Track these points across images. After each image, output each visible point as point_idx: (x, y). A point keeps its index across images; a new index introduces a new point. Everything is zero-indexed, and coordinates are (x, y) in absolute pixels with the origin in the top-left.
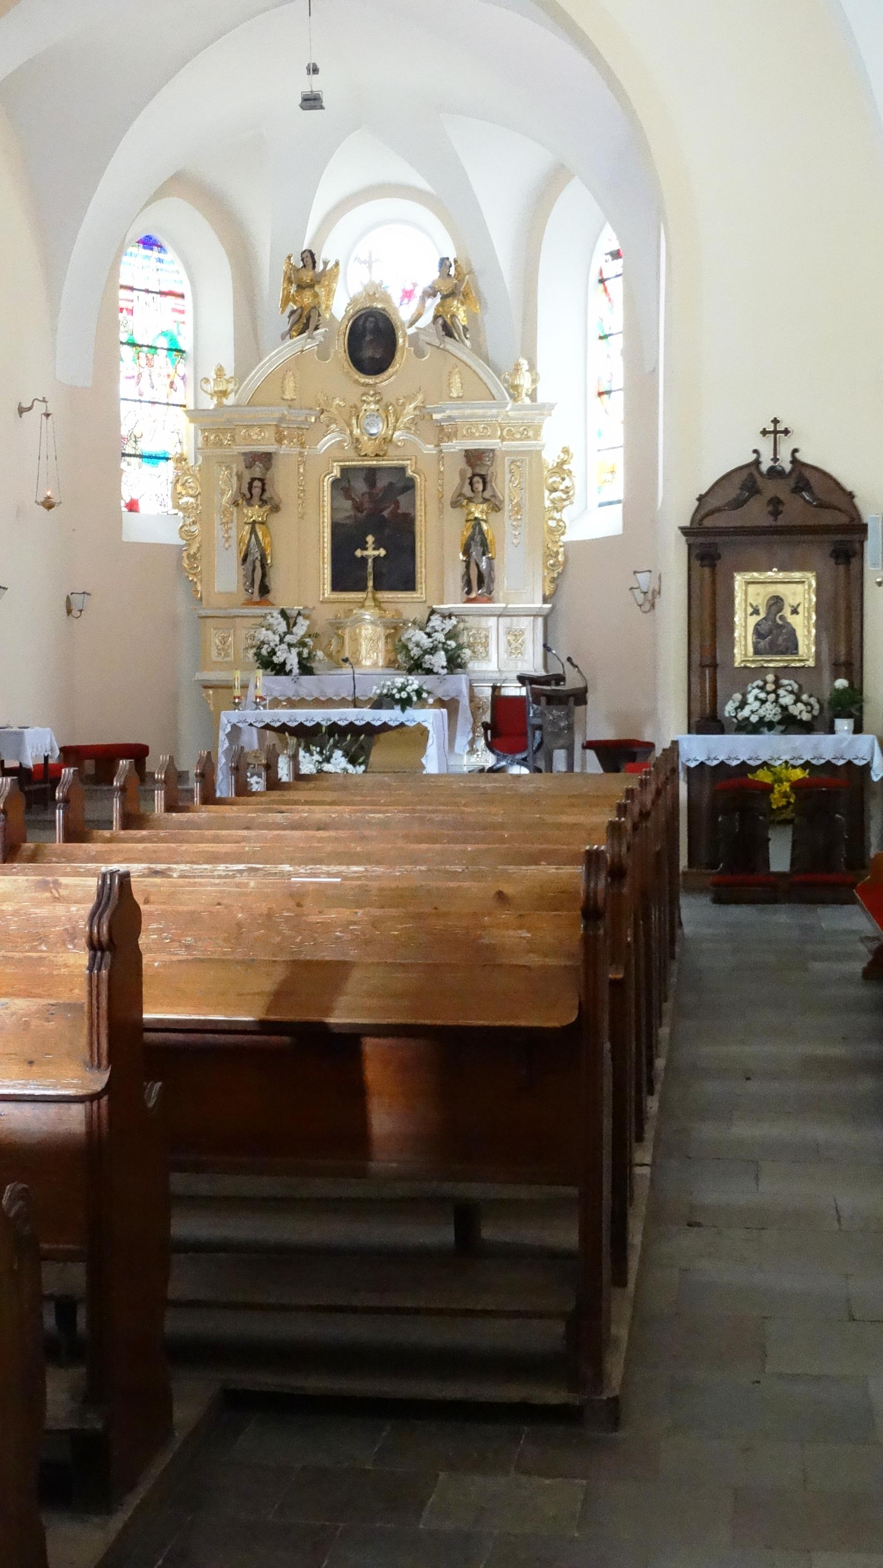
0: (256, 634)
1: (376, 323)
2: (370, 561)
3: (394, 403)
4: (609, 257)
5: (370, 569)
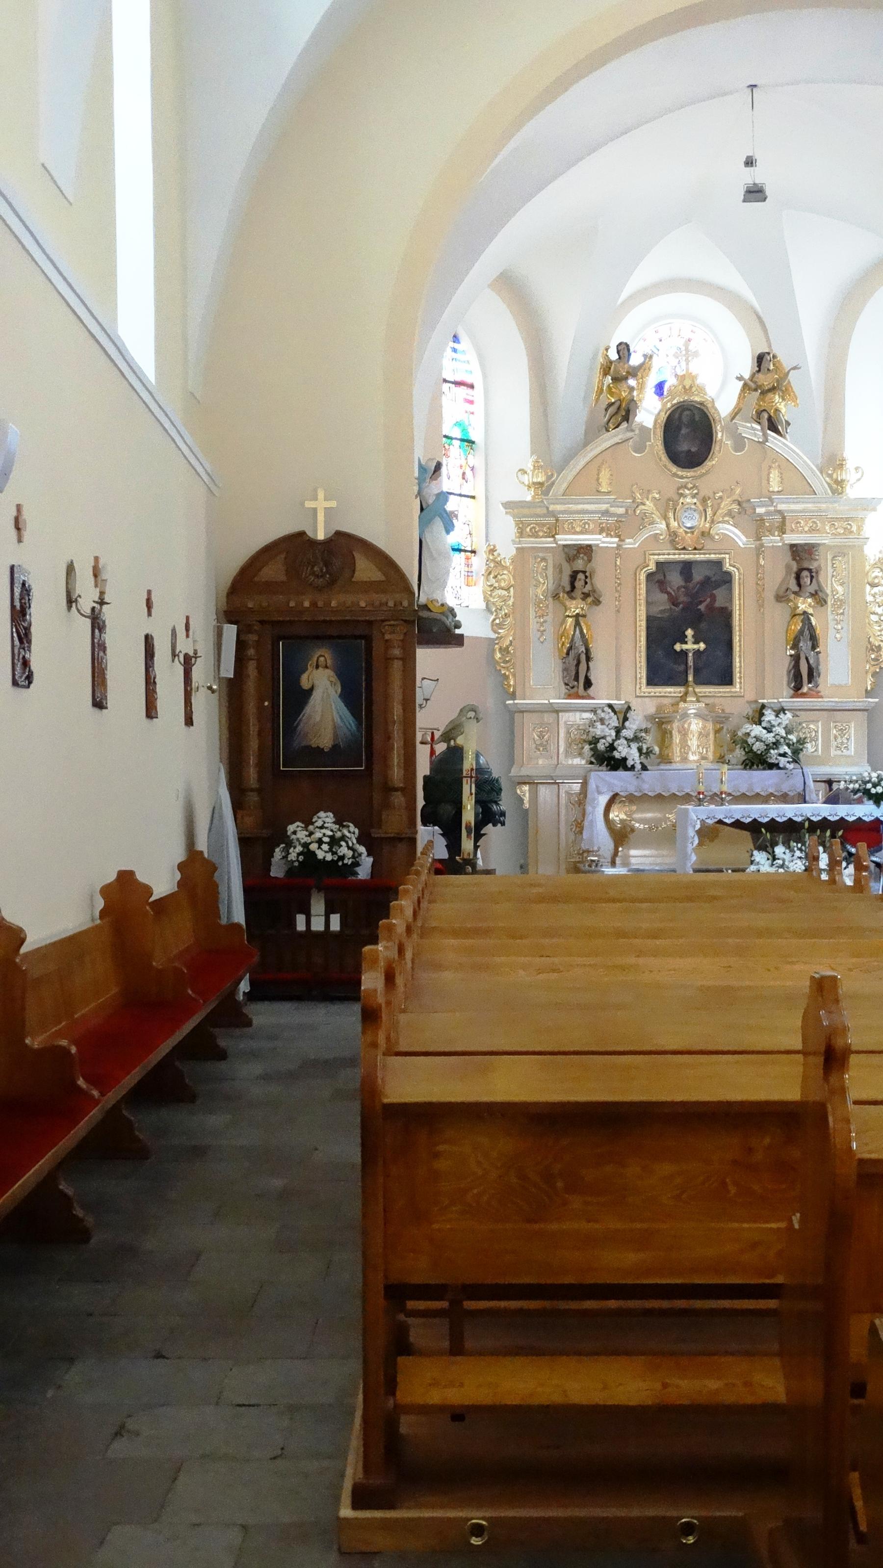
0: (591, 729)
2: (690, 654)
5: (690, 662)
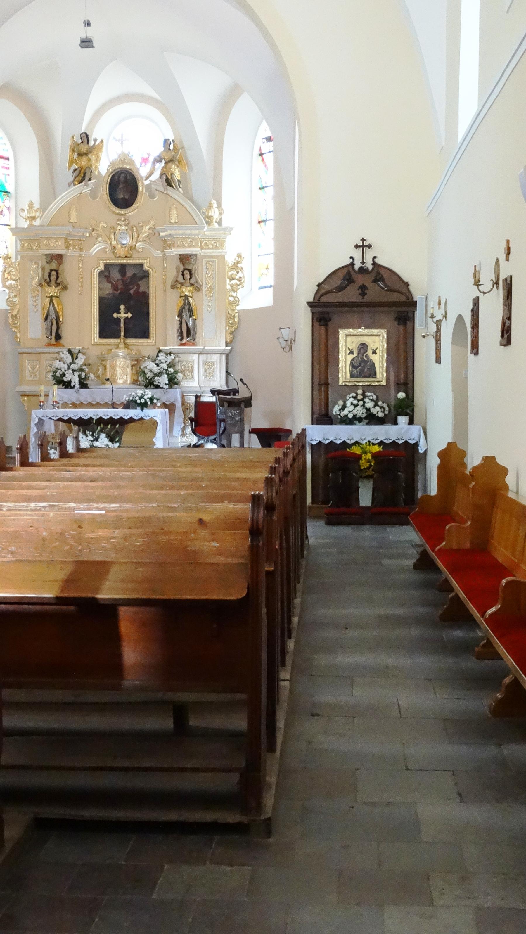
0: (53, 364)
1: (126, 178)
2: (122, 320)
3: (137, 226)
4: (265, 140)
